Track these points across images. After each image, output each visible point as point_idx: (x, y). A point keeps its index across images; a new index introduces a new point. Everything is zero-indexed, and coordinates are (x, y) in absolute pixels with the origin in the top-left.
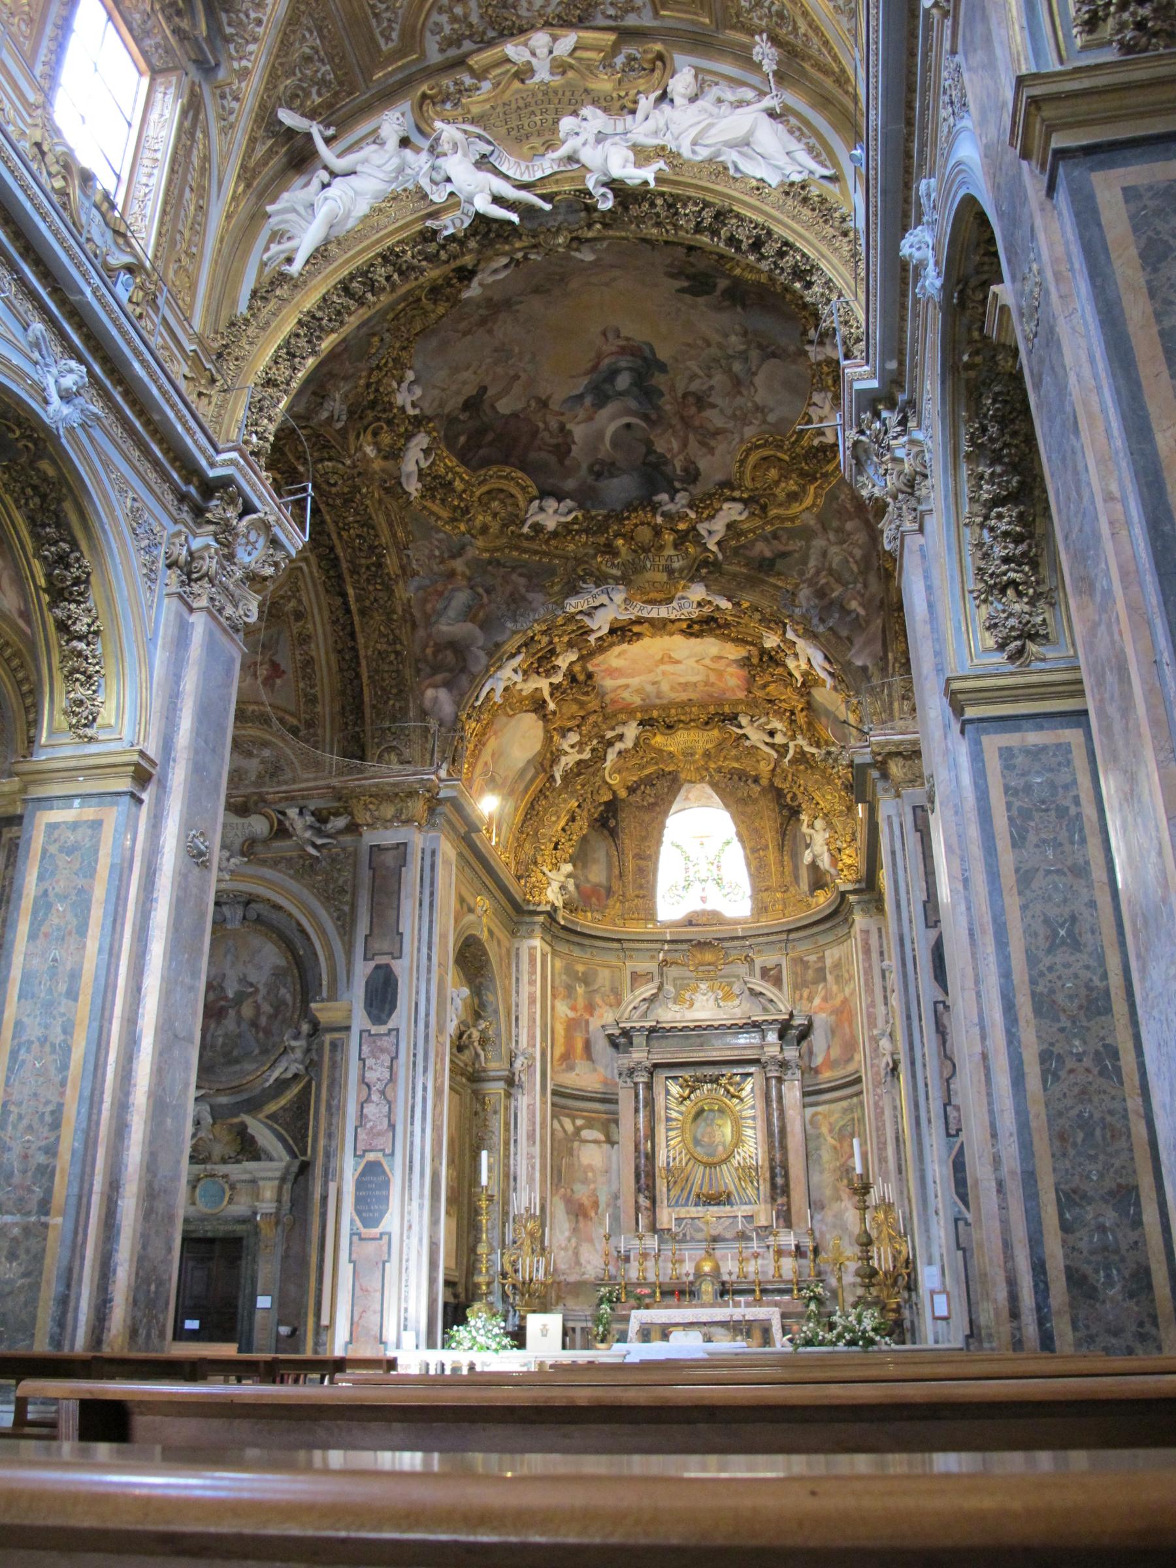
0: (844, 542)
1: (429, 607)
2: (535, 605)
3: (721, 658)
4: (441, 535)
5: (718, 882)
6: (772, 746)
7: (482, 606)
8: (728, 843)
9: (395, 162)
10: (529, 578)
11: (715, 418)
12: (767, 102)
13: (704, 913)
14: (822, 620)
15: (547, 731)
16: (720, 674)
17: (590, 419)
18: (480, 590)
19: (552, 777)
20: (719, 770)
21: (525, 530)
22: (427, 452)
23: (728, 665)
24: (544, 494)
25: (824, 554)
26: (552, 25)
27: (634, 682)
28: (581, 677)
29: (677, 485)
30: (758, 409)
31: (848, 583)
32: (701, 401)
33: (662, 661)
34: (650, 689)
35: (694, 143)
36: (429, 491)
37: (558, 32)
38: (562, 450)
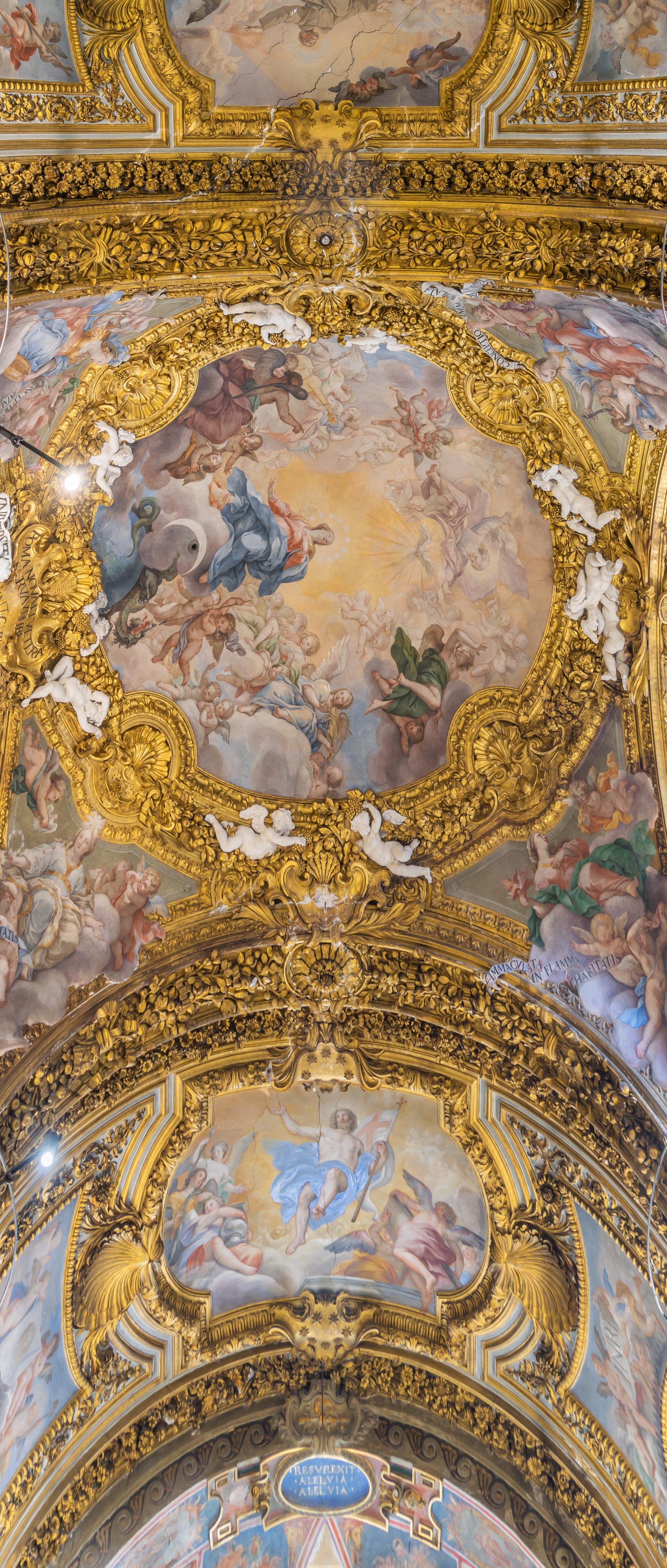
0: (76, 901)
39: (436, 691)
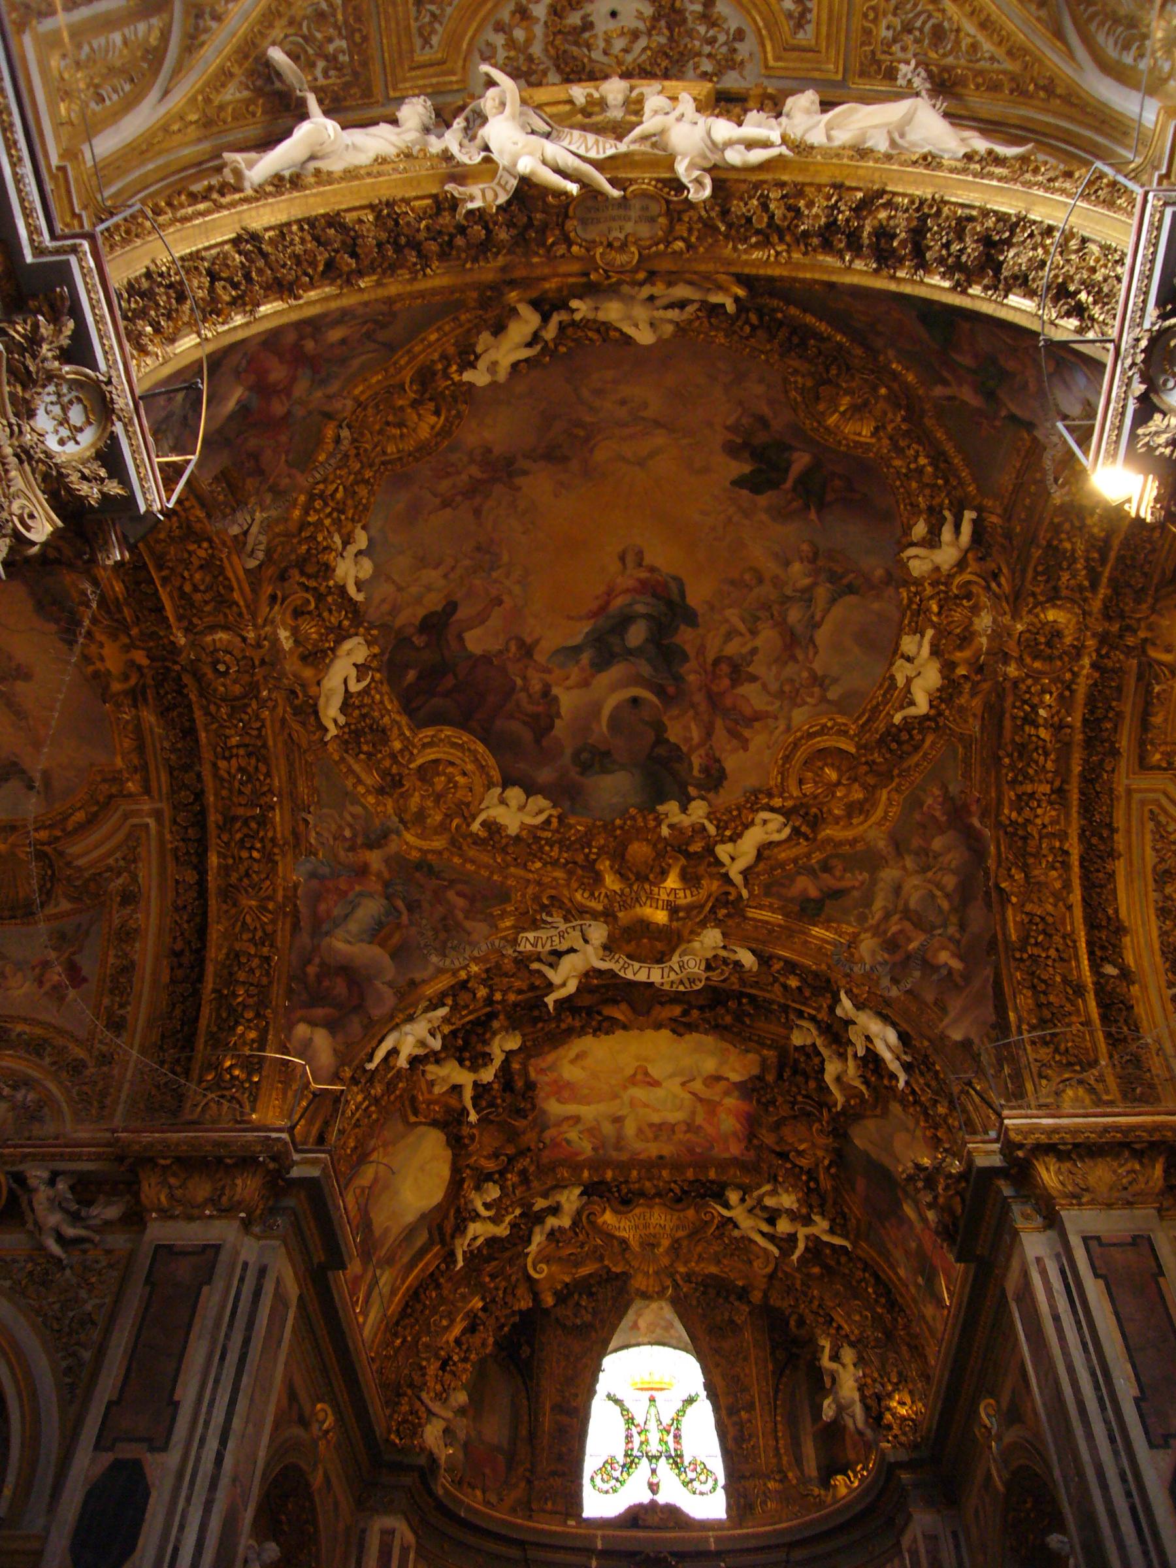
0: (929, 868)
1: (323, 907)
2: (475, 937)
3: (718, 1078)
4: (358, 810)
5: (676, 1460)
6: (771, 1238)
7: (399, 926)
8: (690, 1401)
10: (472, 900)
11: (752, 696)
13: (653, 1503)
14: (895, 981)
15: (456, 1169)
16: (711, 1107)
17: (585, 683)
18: (400, 904)
19: (452, 1254)
20: (688, 1277)
21: (476, 827)
22: (361, 669)
23: (727, 1093)
24: (507, 782)
25: (897, 890)
27: (588, 1112)
28: (519, 1084)
29: (692, 791)
30: (817, 680)
31: (934, 928)
32: (738, 672)
33: (632, 1080)
34: (608, 1129)
36: (352, 737)
38: (542, 724)
39: (796, 455)
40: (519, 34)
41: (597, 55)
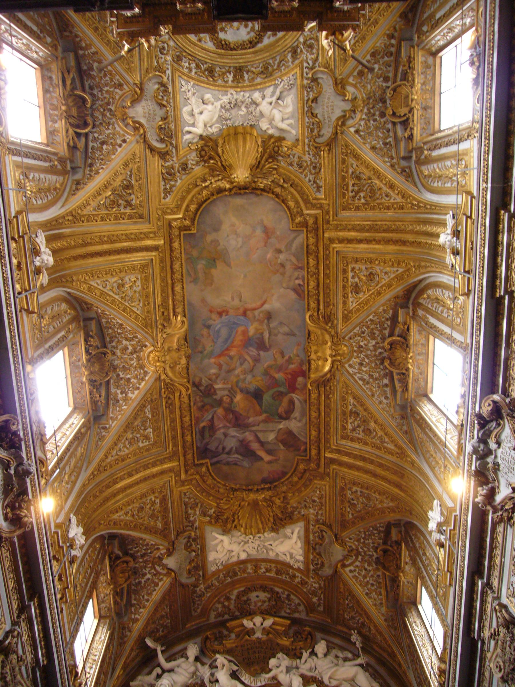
9: (192, 669)
12: (359, 661)
26: (263, 613)
35: (330, 678)
37: (265, 616)
40: (226, 603)
41: (252, 607)
